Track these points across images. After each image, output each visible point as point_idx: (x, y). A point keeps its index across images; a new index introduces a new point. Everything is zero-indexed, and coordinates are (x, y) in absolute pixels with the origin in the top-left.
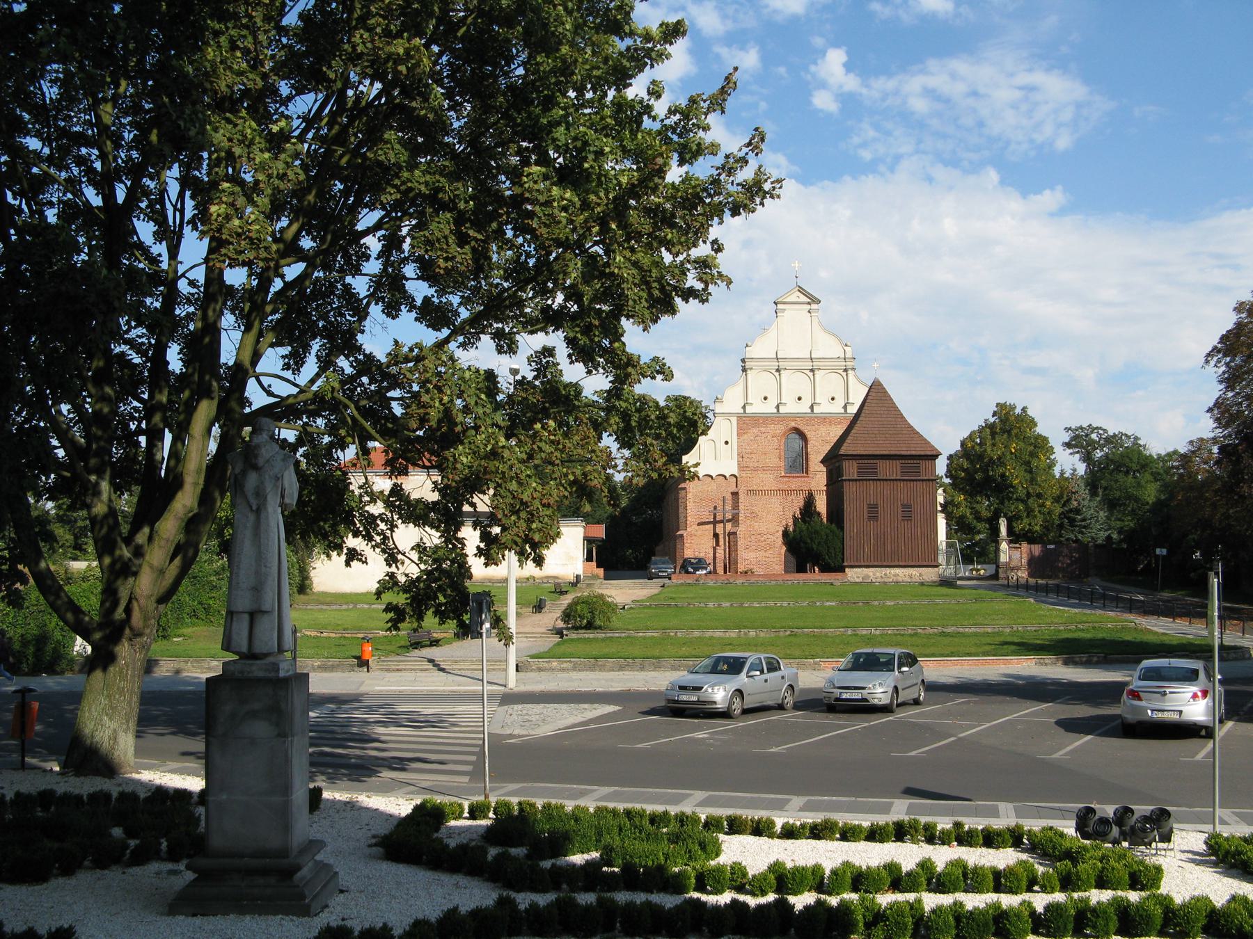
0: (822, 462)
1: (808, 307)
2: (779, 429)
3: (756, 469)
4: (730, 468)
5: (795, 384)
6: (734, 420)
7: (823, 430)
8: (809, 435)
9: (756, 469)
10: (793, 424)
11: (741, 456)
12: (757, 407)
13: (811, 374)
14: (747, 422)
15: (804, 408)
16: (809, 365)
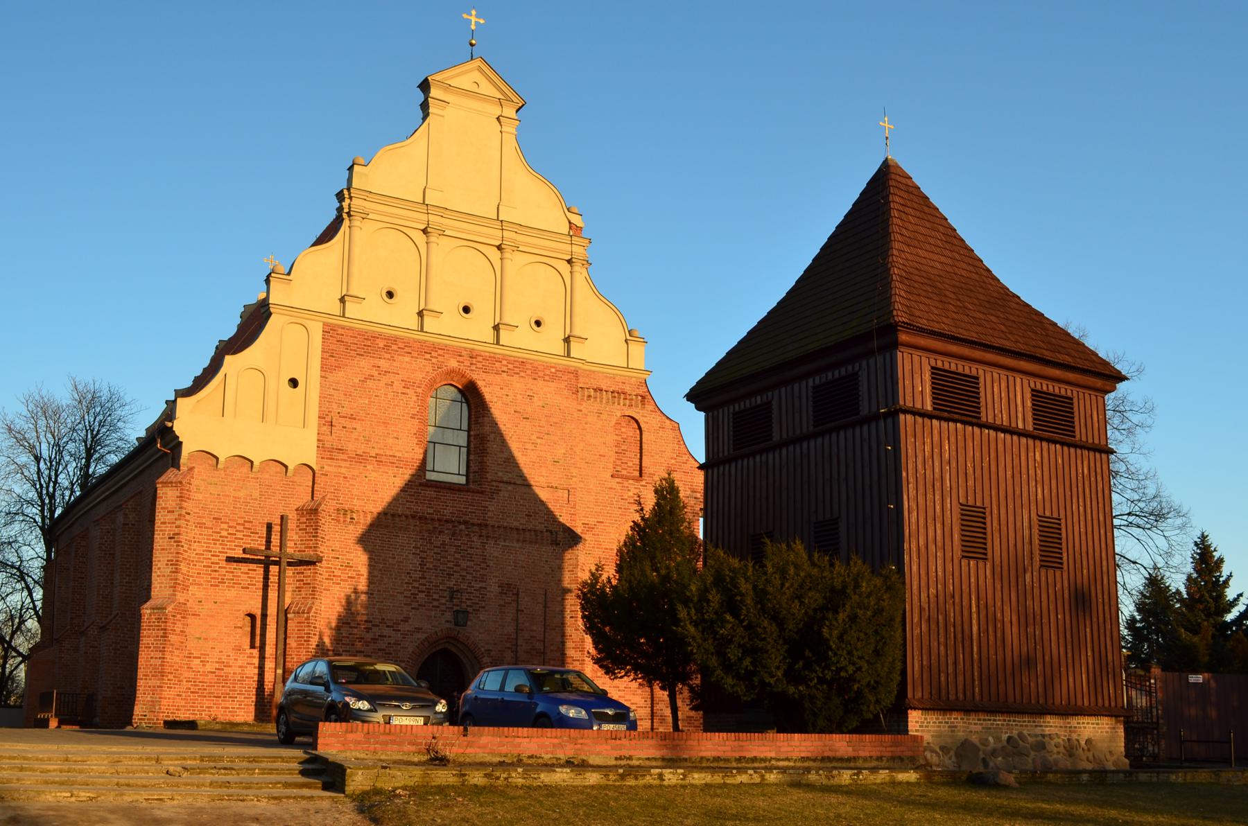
0: (697, 396)
1: (497, 111)
2: (420, 370)
3: (361, 459)
4: (300, 447)
5: (460, 273)
6: (317, 329)
7: (518, 385)
8: (489, 393)
9: (361, 459)
10: (453, 364)
11: (326, 421)
12: (371, 312)
13: (494, 255)
14: (345, 344)
15: (477, 330)
16: (495, 236)
